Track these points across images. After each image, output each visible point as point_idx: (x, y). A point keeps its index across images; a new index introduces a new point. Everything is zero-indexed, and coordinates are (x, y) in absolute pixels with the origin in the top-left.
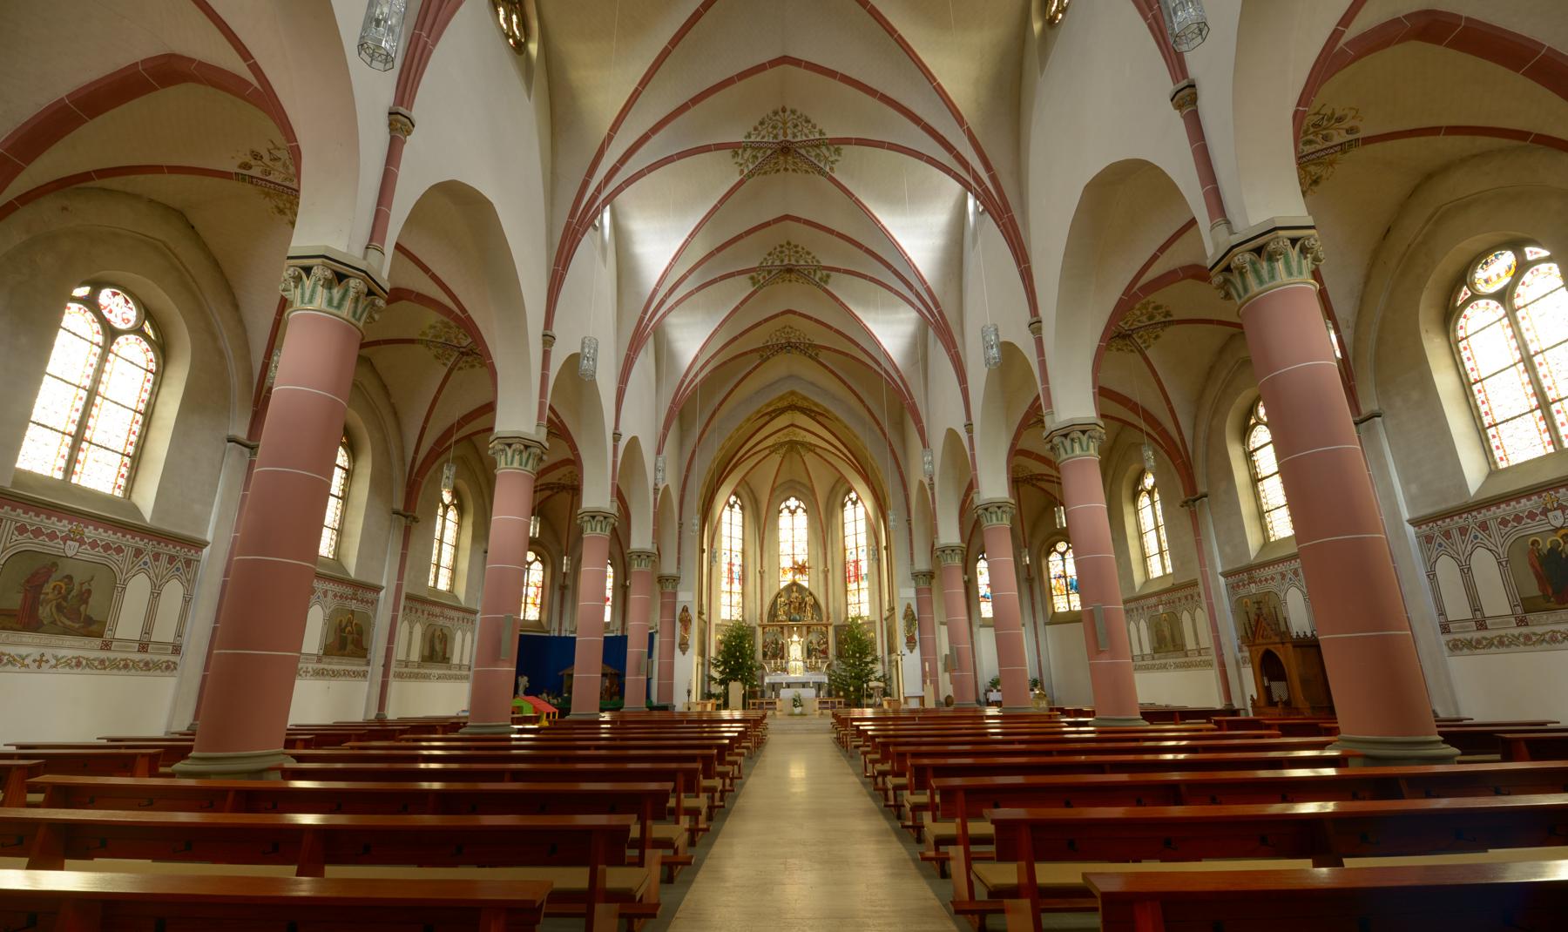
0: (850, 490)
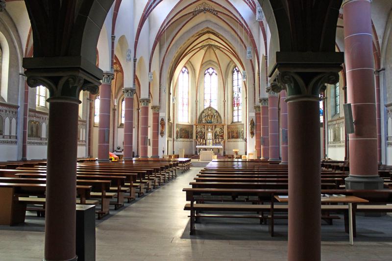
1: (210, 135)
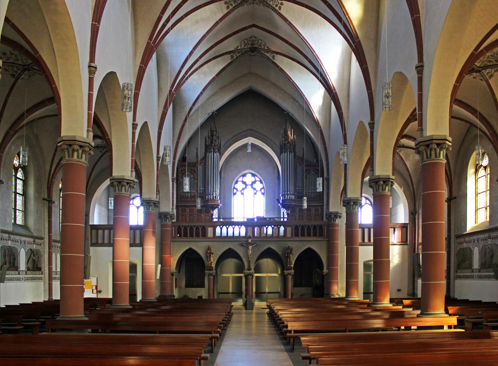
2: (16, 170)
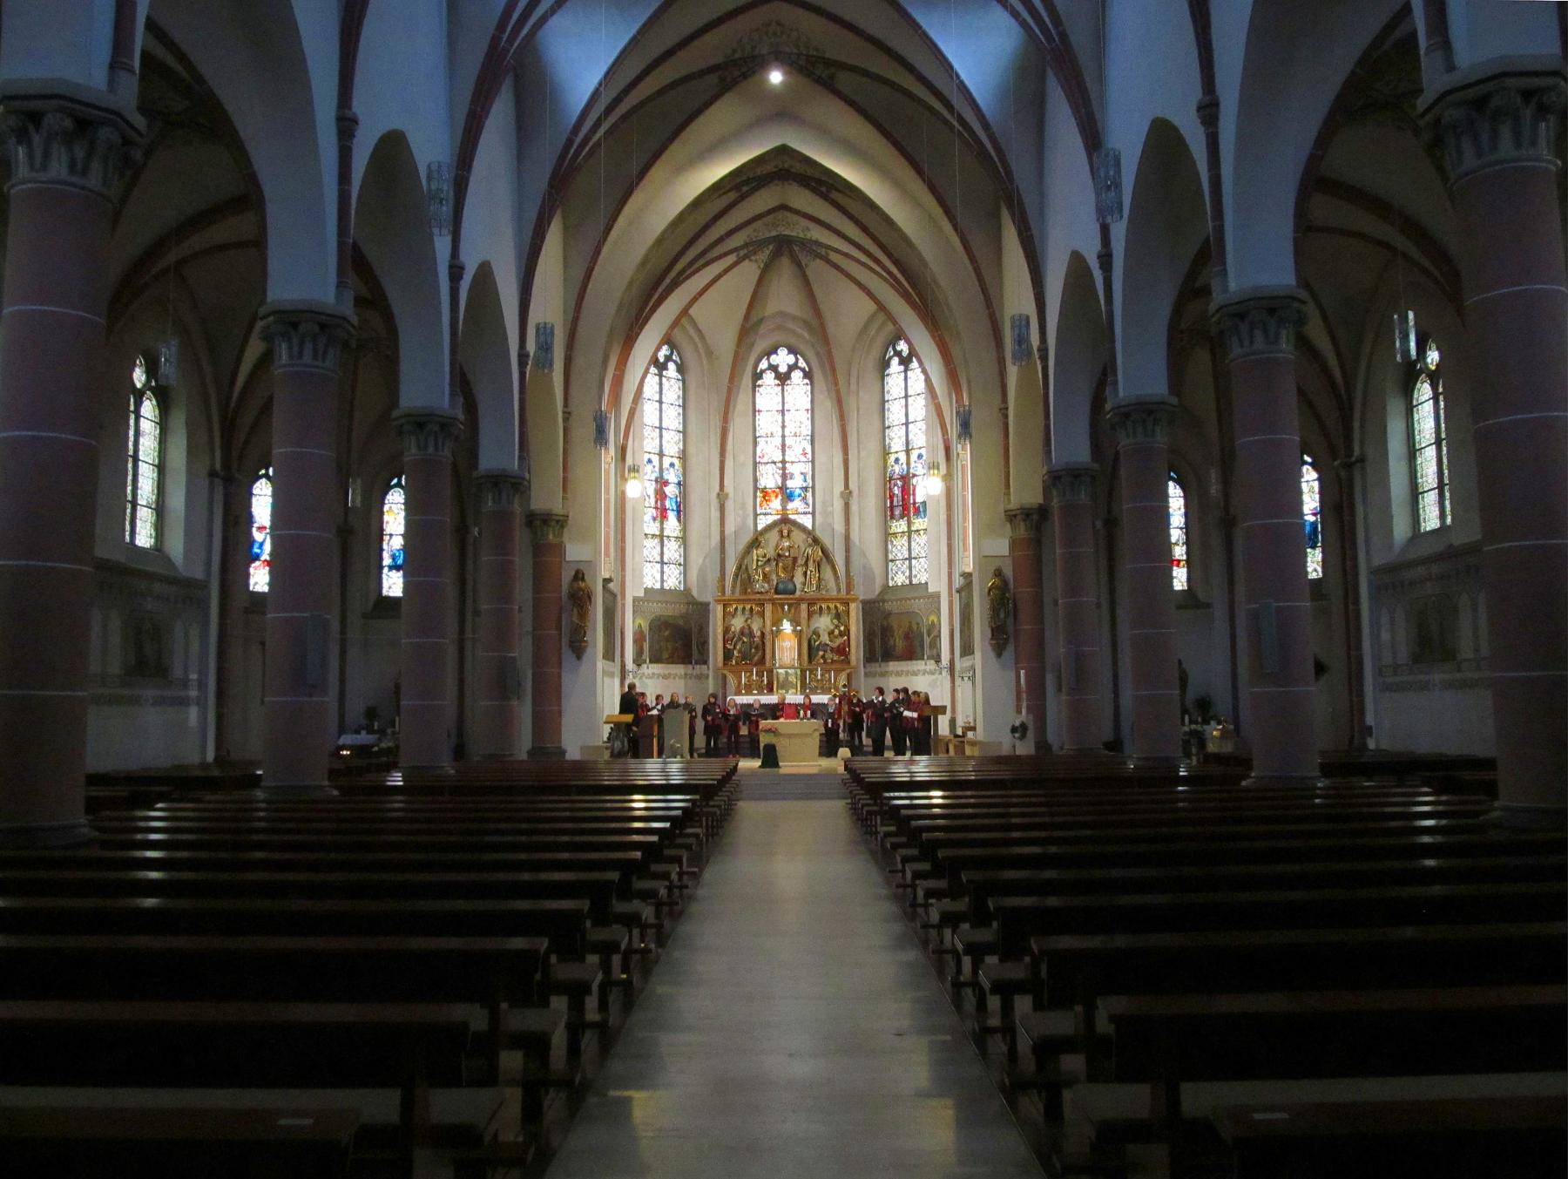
0: (899, 335)
1: (787, 648)
2: (139, 396)
